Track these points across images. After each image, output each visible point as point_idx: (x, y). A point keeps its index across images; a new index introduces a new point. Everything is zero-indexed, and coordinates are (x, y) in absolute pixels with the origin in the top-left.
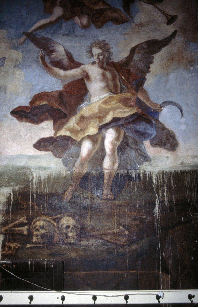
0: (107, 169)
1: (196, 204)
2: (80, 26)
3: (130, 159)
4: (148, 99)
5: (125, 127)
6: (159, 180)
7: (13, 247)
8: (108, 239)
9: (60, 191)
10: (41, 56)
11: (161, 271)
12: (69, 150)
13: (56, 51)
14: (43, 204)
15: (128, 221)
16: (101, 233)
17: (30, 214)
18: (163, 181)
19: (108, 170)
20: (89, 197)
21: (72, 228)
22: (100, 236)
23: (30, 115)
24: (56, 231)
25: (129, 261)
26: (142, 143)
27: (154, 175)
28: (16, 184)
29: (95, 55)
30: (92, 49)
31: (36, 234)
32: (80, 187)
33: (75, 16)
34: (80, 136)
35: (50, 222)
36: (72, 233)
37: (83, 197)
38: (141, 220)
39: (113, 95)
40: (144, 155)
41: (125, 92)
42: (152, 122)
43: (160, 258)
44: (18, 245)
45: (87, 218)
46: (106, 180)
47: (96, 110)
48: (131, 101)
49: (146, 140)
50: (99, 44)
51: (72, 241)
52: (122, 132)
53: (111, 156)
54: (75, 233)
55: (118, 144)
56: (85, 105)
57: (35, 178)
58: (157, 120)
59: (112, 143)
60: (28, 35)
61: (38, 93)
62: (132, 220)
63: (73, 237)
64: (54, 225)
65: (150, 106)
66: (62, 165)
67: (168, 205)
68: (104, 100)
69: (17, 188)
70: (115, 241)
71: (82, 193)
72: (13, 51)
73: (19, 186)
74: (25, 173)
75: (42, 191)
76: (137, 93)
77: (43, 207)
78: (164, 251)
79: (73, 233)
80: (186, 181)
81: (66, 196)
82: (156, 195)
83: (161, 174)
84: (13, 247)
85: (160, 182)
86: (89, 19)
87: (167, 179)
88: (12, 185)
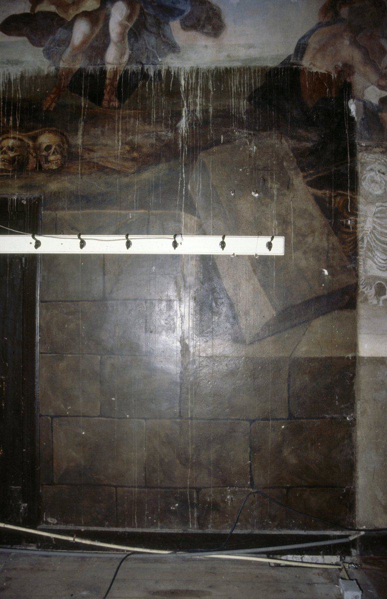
0: (110, 64)
1: (245, 117)
3: (146, 48)
14: (14, 115)
18: (197, 83)
19: (113, 64)
21: (55, 149)
26: (168, 24)
36: (54, 156)
38: (159, 138)
40: (170, 43)
43: (184, 193)
49: (174, 20)
52: (138, 7)
53: (119, 44)
55: (130, 25)
59: (121, 24)
62: (146, 137)
67: (200, 117)
75: (12, 95)
80: (232, 84)
82: (183, 101)
85: (192, 83)
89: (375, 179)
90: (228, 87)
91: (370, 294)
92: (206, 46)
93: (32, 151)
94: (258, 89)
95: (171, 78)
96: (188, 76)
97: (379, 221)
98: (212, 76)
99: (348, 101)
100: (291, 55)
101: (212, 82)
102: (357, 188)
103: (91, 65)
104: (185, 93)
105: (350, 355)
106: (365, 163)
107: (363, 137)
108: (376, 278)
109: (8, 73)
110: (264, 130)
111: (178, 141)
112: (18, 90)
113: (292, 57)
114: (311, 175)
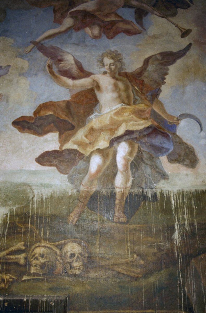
0: (119, 188)
2: (91, 37)
3: (145, 176)
4: (164, 111)
5: (139, 141)
7: (6, 279)
8: (120, 270)
9: (64, 212)
10: (48, 65)
12: (76, 165)
13: (64, 60)
14: (45, 228)
15: (143, 248)
16: (111, 262)
17: (29, 239)
18: (184, 202)
19: (121, 188)
20: (99, 220)
21: (78, 257)
22: (110, 267)
23: (34, 126)
24: (58, 260)
25: (145, 297)
26: (158, 158)
27: (172, 195)
28: (14, 203)
29: (106, 65)
30: (103, 59)
31: (34, 263)
32: (88, 207)
33: (86, 27)
34: (89, 150)
35: (52, 249)
36: (77, 263)
37: (91, 219)
38: (159, 248)
39: (126, 107)
40: (161, 172)
41: (139, 104)
43: (182, 294)
44: (13, 277)
45: (95, 244)
46: (118, 200)
47: (107, 122)
48: (145, 112)
49: (163, 155)
50: (110, 54)
51: (78, 272)
52: (136, 146)
53: (124, 173)
54: (81, 263)
55: (132, 159)
56: (94, 116)
57: (36, 196)
58: (174, 134)
59: (125, 158)
60: (36, 44)
61: (43, 103)
62: (148, 247)
63: (79, 267)
64: (56, 253)
65: (166, 119)
66: (68, 182)
67: (189, 229)
68: (116, 111)
69: (14, 208)
70: (128, 273)
71: (90, 215)
72: (19, 60)
73: (17, 206)
74: (25, 190)
76: (152, 105)
77: (44, 231)
78: (186, 285)
79: (79, 262)
81: (72, 218)
82: (175, 218)
83: (181, 194)
84: (6, 280)
85: (180, 203)
86: (100, 30)
87: (187, 199)
88: (9, 204)
93: (59, 258)
95: (164, 200)
101: (194, 202)
103: (104, 189)
109: (41, 193)
111: (174, 250)
112: (48, 206)
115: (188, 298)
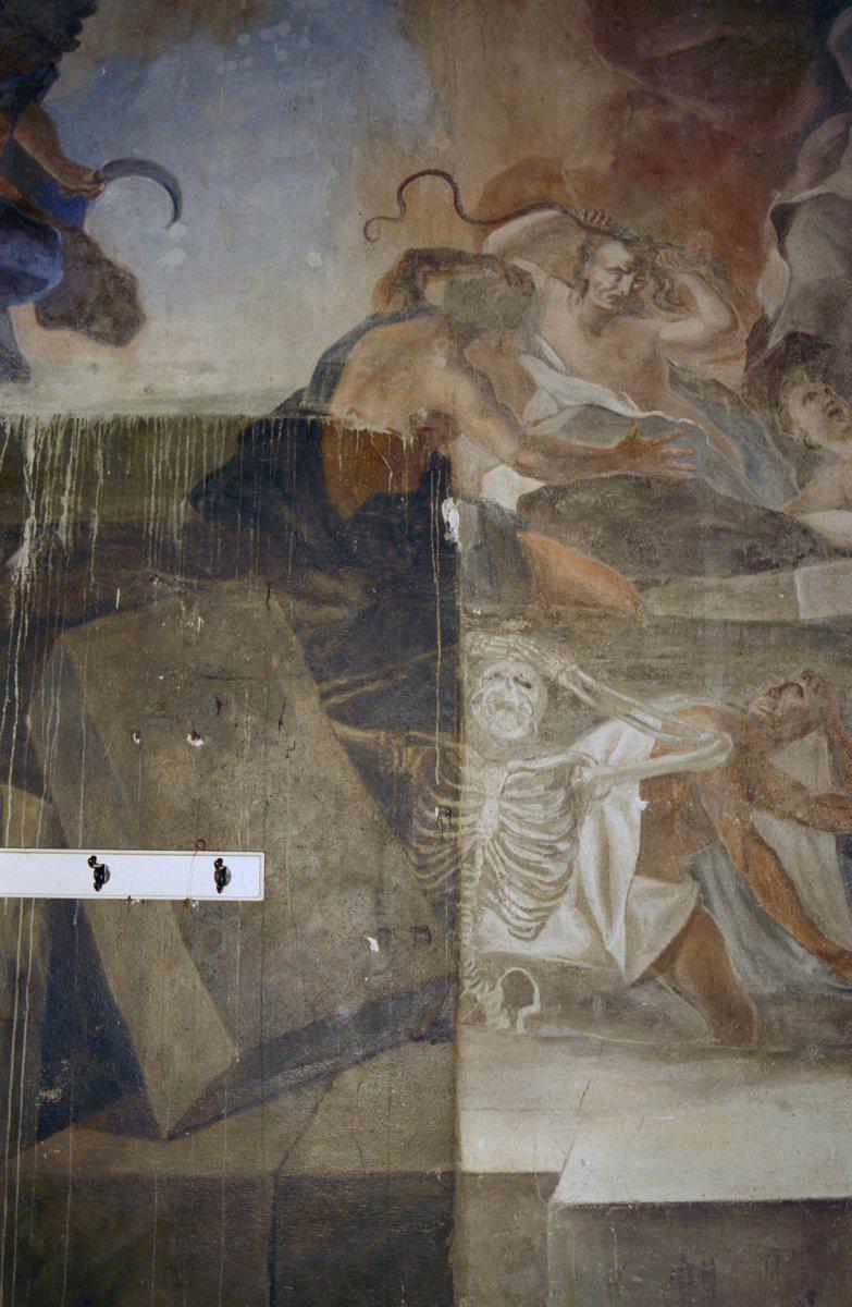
1: (180, 542)
4: (53, 151)
6: (51, 450)
11: (12, 781)
18: (66, 454)
27: (31, 431)
42: (53, 235)
43: (14, 736)
58: (75, 230)
65: (55, 176)
76: (13, 128)
78: (30, 709)
80: (154, 462)
85: (53, 456)
87: (81, 446)
89: (506, 699)
90: (143, 468)
91: (490, 1003)
92: (94, 365)
94: (218, 471)
95: (3, 443)
96: (46, 439)
97: (515, 809)
98: (104, 442)
99: (441, 503)
100: (302, 391)
101: (104, 455)
102: (458, 724)
104: (34, 478)
105: (438, 1170)
106: (481, 658)
107: (477, 592)
108: (506, 958)
110: (226, 575)
111: (8, 602)
113: (306, 394)
114: (340, 690)
115: (32, 749)
